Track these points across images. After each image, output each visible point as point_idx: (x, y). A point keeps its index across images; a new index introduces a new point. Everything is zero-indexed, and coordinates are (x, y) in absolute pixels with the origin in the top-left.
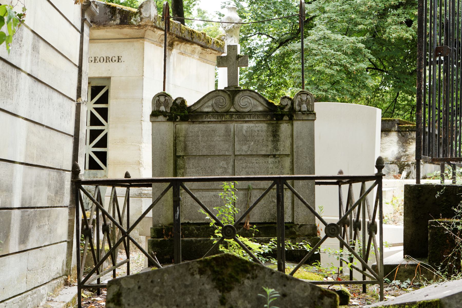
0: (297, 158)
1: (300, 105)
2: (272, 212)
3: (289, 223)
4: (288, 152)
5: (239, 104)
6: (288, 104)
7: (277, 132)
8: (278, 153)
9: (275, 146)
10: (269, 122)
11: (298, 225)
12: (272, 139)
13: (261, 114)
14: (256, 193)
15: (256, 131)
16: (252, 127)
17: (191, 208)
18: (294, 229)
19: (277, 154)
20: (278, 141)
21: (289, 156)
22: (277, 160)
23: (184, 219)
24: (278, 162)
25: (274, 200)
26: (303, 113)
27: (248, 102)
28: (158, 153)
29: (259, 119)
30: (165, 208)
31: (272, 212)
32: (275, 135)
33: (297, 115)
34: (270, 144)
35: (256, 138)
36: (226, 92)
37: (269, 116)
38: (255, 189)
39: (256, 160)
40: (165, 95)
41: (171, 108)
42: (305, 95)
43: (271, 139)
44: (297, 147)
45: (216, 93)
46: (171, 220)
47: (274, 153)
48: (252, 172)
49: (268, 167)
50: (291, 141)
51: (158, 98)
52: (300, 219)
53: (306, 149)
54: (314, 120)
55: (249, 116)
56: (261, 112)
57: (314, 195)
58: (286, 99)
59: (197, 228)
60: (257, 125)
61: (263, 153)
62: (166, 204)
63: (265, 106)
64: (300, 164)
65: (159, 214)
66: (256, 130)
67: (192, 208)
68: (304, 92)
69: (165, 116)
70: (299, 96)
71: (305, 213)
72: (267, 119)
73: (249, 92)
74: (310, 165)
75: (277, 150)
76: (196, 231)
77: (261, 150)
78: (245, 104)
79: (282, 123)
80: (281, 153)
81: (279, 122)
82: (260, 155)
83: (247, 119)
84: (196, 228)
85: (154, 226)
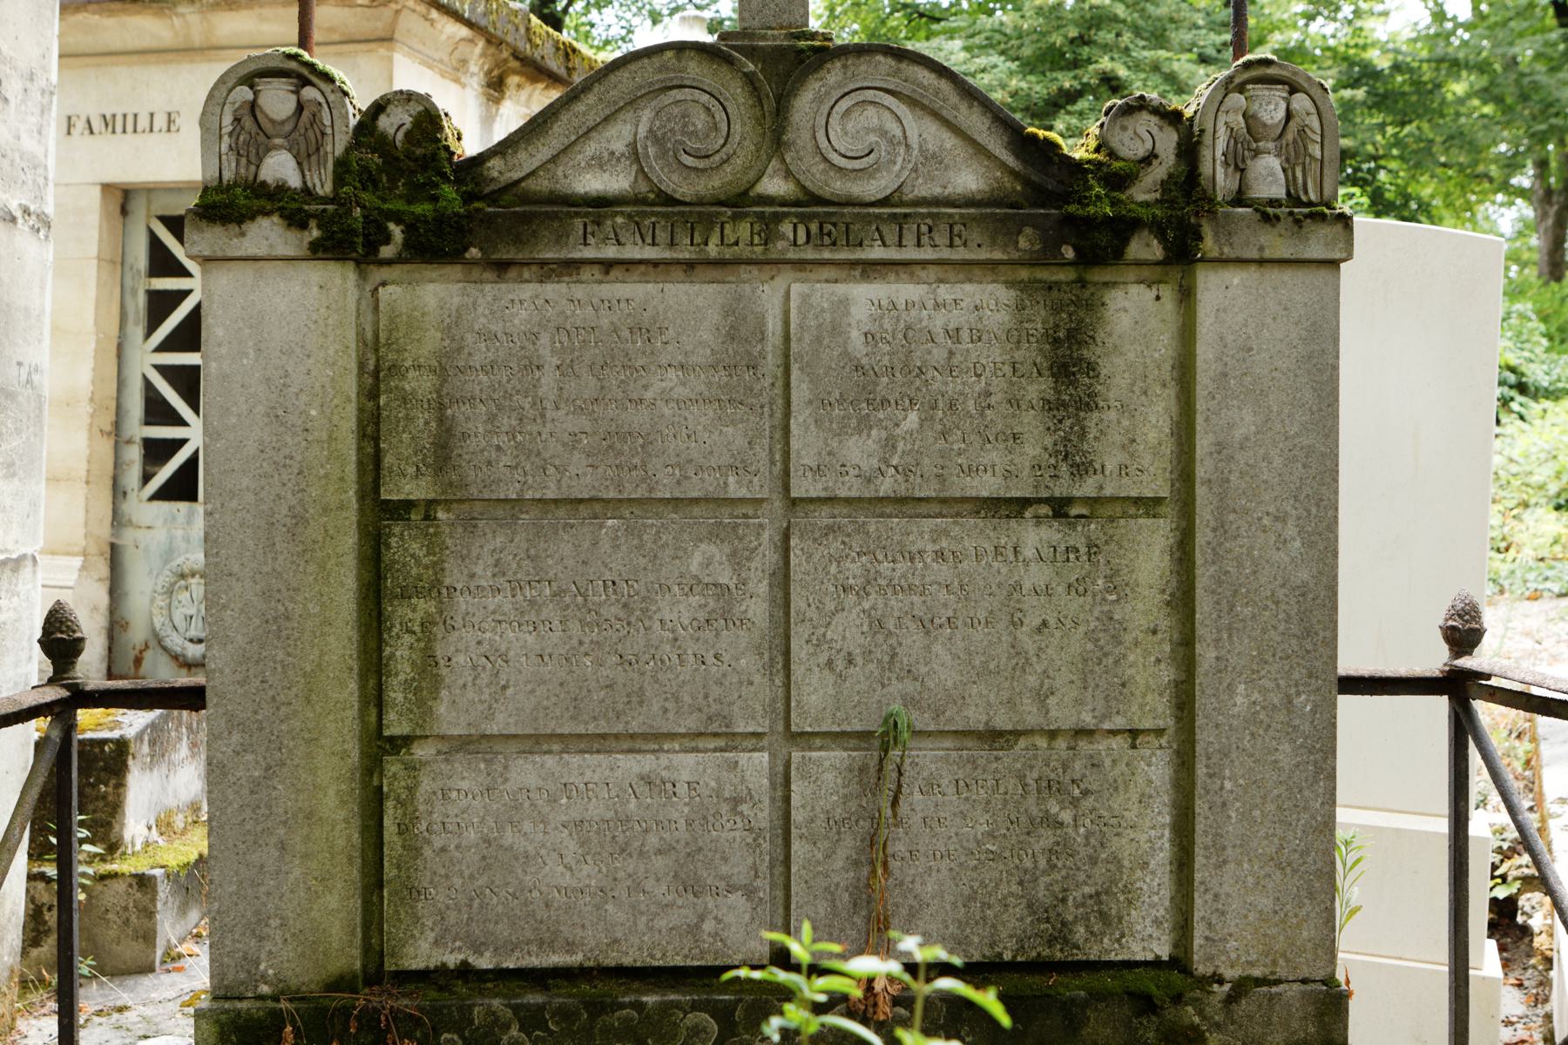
0: (1220, 527)
1: (1237, 163)
2: (1042, 893)
3: (1157, 963)
4: (1156, 483)
5: (823, 143)
6: (1159, 149)
7: (1080, 344)
8: (1088, 488)
9: (1066, 439)
10: (1024, 274)
11: (1221, 981)
12: (1051, 395)
13: (974, 218)
14: (935, 760)
15: (941, 338)
16: (909, 305)
17: (486, 865)
18: (1190, 1014)
19: (1077, 493)
20: (1088, 403)
21: (1163, 509)
22: (1077, 539)
23: (436, 943)
24: (1083, 550)
25: (1055, 809)
26: (1267, 214)
27: (883, 133)
28: (245, 482)
29: (960, 254)
30: (297, 872)
31: (1042, 893)
32: (1065, 366)
33: (1226, 230)
34: (1031, 423)
35: (936, 386)
36: (729, 61)
37: (1028, 230)
38: (930, 734)
39: (937, 535)
40: (300, 76)
41: (342, 165)
42: (1280, 92)
43: (1038, 388)
44: (1220, 447)
45: (663, 68)
46: (346, 956)
47: (1060, 490)
48: (907, 621)
49: (1018, 587)
50: (1174, 409)
51: (245, 93)
52: (1232, 944)
53: (1278, 462)
54: (1334, 264)
55: (890, 232)
56: (970, 202)
57: (1332, 777)
58: (1145, 115)
59: (527, 1007)
60: (946, 293)
61: (987, 486)
62: (307, 839)
63: (1003, 165)
64: (1240, 565)
65: (257, 913)
66: (938, 330)
67: (488, 867)
68: (1271, 71)
69: (296, 220)
70: (1236, 99)
71: (1266, 903)
72: (1016, 255)
73: (891, 62)
74: (1304, 575)
75: (1081, 469)
76: (514, 1032)
77: (971, 470)
78: (860, 148)
79: (1115, 284)
80: (1108, 492)
81: (1097, 275)
82: (964, 500)
83: (877, 252)
84: (516, 1009)
85: (222, 992)
